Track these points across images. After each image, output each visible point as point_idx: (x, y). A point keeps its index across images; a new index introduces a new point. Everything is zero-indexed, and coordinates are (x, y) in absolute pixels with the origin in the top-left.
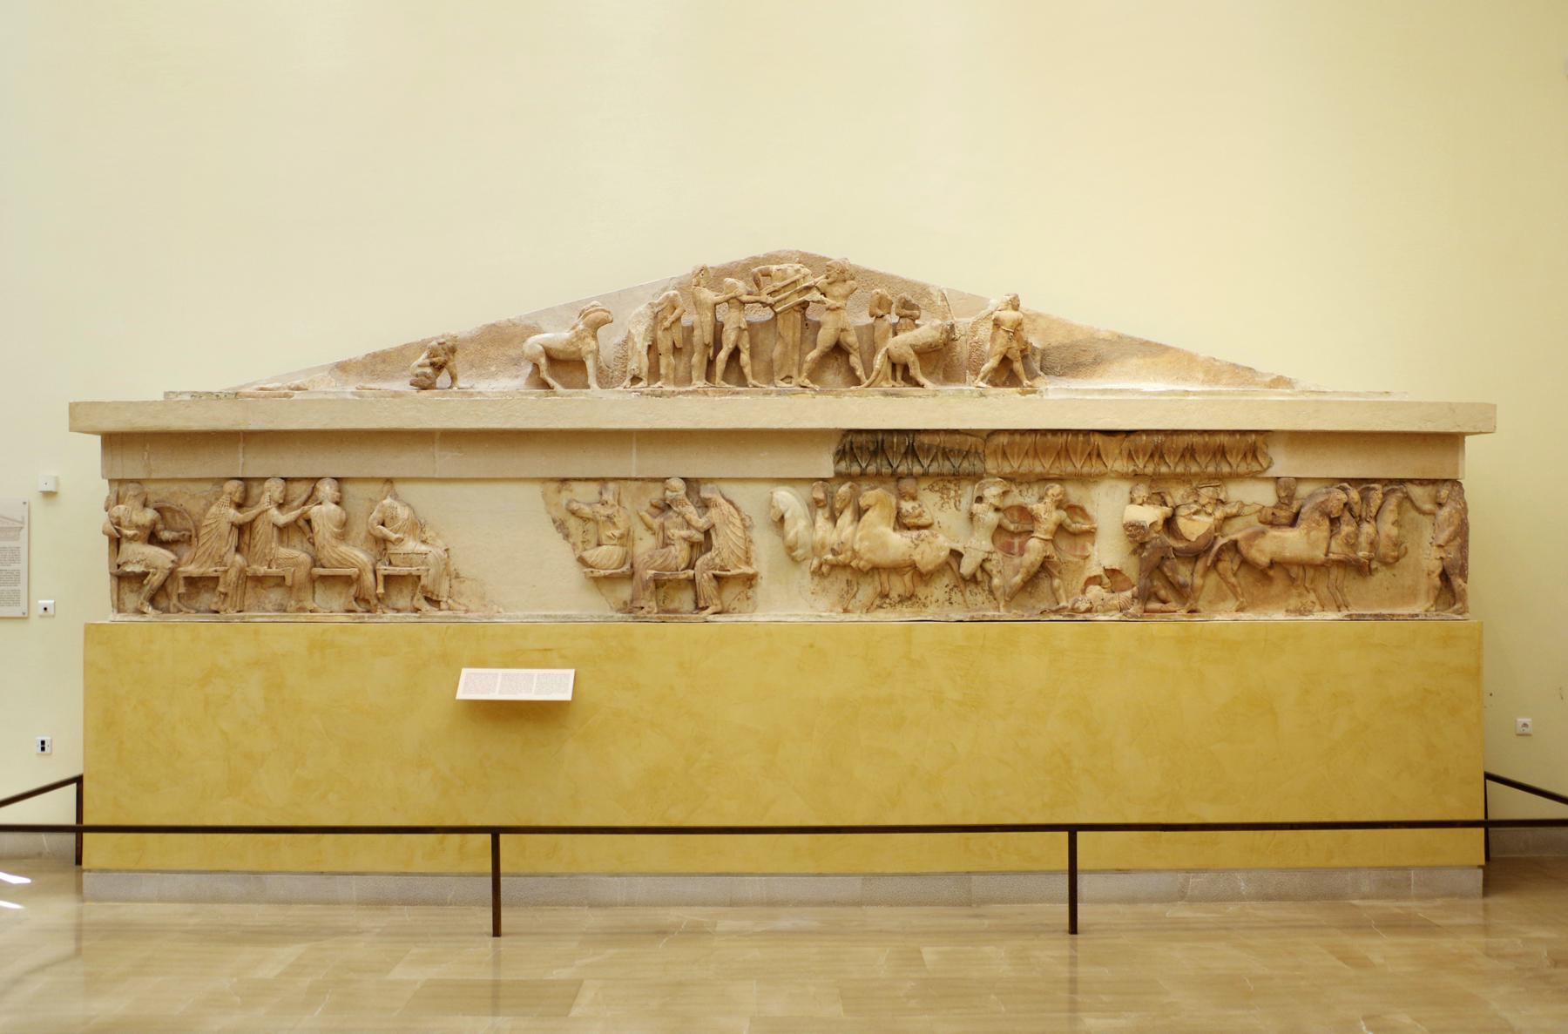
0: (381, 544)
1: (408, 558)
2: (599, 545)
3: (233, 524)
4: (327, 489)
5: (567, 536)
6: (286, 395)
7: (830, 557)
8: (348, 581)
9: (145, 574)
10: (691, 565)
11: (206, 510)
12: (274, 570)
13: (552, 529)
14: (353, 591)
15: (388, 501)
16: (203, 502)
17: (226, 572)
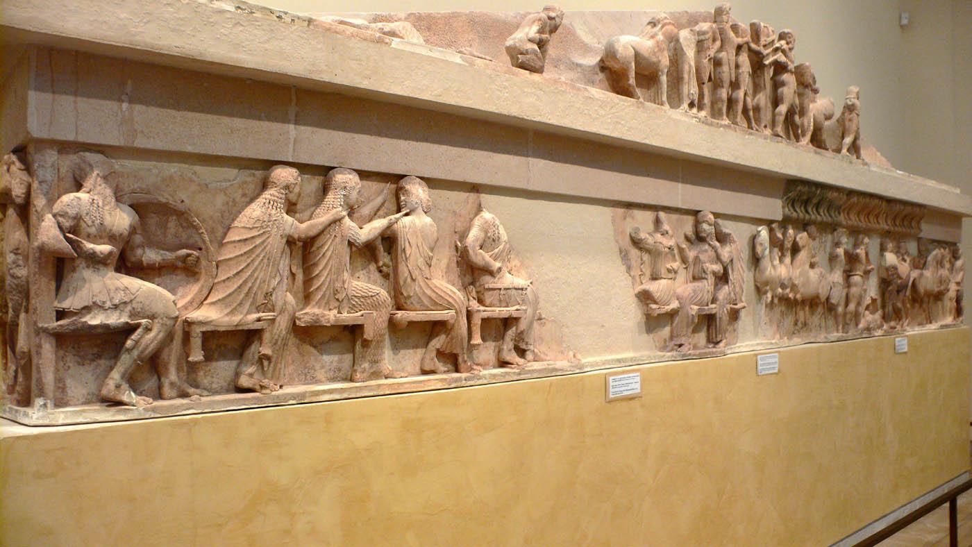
0: (472, 272)
1: (506, 296)
2: (655, 278)
3: (290, 242)
4: (418, 192)
5: (629, 268)
6: (379, 41)
7: (780, 290)
8: (436, 328)
9: (129, 330)
10: (714, 301)
11: (234, 210)
12: (347, 317)
13: (619, 262)
14: (438, 342)
15: (487, 215)
16: (220, 200)
17: (273, 321)
